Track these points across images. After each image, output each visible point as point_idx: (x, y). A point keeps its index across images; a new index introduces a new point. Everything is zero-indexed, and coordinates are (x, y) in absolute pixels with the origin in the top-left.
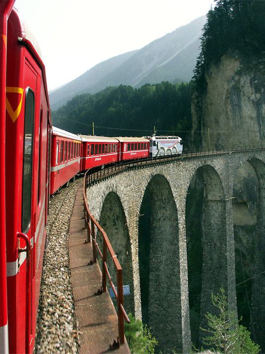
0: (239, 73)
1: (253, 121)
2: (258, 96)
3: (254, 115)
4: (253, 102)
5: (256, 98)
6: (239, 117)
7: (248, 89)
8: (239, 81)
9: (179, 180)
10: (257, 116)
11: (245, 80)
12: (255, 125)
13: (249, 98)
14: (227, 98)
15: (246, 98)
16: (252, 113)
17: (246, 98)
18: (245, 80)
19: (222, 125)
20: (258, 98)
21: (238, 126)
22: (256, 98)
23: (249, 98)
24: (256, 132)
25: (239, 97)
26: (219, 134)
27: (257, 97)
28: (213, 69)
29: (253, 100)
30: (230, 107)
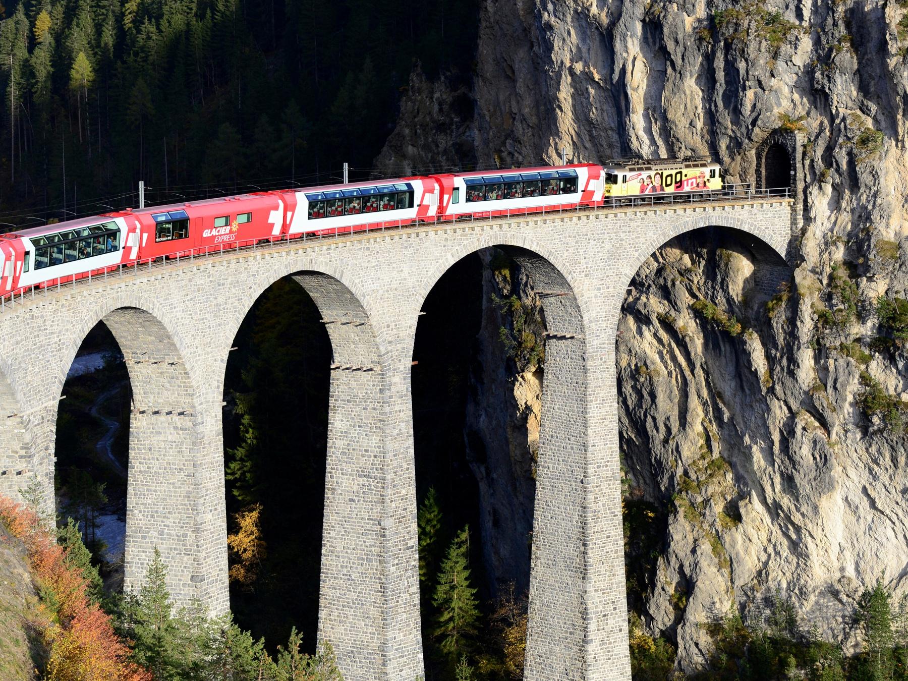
19: (520, 84)
24: (611, 129)
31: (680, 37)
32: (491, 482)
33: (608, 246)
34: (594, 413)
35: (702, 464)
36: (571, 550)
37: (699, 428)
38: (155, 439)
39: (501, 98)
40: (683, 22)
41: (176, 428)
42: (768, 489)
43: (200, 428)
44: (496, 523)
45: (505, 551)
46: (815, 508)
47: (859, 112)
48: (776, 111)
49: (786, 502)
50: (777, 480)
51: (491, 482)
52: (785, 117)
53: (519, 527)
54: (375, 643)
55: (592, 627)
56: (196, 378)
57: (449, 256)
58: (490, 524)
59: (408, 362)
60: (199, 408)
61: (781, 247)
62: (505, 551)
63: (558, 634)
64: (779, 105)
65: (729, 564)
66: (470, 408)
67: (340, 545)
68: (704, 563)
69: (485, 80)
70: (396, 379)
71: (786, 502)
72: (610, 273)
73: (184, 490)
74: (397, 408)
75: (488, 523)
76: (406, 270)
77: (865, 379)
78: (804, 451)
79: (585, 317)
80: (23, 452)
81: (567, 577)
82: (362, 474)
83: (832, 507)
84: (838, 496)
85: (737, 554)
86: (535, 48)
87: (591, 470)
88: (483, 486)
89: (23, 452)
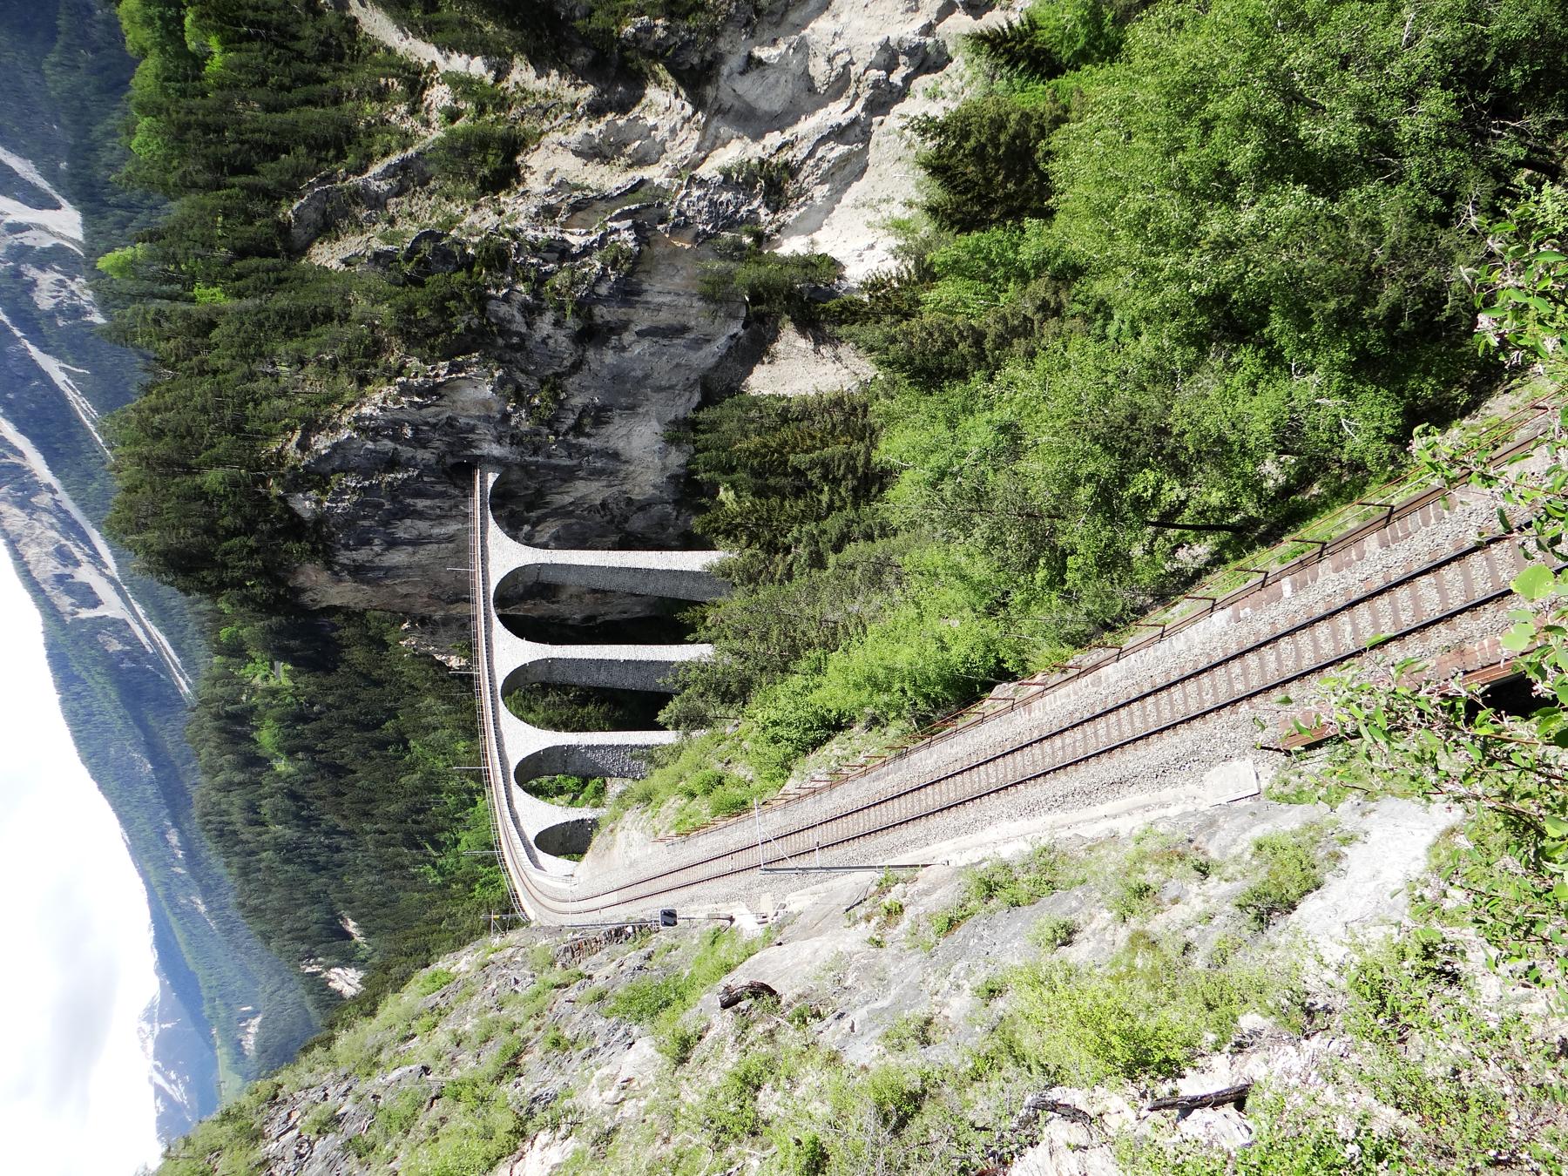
0: (329, 565)
2: (376, 541)
3: (410, 549)
4: (386, 550)
7: (362, 555)
8: (343, 566)
9: (522, 739)
11: (344, 557)
13: (378, 555)
14: (368, 583)
18: (344, 557)
23: (378, 555)
25: (373, 569)
26: (429, 596)
28: (306, 598)
30: (388, 582)
46: (626, 462)
49: (622, 475)
59: (548, 647)
71: (622, 475)
77: (566, 434)
78: (599, 465)
88: (608, 618)
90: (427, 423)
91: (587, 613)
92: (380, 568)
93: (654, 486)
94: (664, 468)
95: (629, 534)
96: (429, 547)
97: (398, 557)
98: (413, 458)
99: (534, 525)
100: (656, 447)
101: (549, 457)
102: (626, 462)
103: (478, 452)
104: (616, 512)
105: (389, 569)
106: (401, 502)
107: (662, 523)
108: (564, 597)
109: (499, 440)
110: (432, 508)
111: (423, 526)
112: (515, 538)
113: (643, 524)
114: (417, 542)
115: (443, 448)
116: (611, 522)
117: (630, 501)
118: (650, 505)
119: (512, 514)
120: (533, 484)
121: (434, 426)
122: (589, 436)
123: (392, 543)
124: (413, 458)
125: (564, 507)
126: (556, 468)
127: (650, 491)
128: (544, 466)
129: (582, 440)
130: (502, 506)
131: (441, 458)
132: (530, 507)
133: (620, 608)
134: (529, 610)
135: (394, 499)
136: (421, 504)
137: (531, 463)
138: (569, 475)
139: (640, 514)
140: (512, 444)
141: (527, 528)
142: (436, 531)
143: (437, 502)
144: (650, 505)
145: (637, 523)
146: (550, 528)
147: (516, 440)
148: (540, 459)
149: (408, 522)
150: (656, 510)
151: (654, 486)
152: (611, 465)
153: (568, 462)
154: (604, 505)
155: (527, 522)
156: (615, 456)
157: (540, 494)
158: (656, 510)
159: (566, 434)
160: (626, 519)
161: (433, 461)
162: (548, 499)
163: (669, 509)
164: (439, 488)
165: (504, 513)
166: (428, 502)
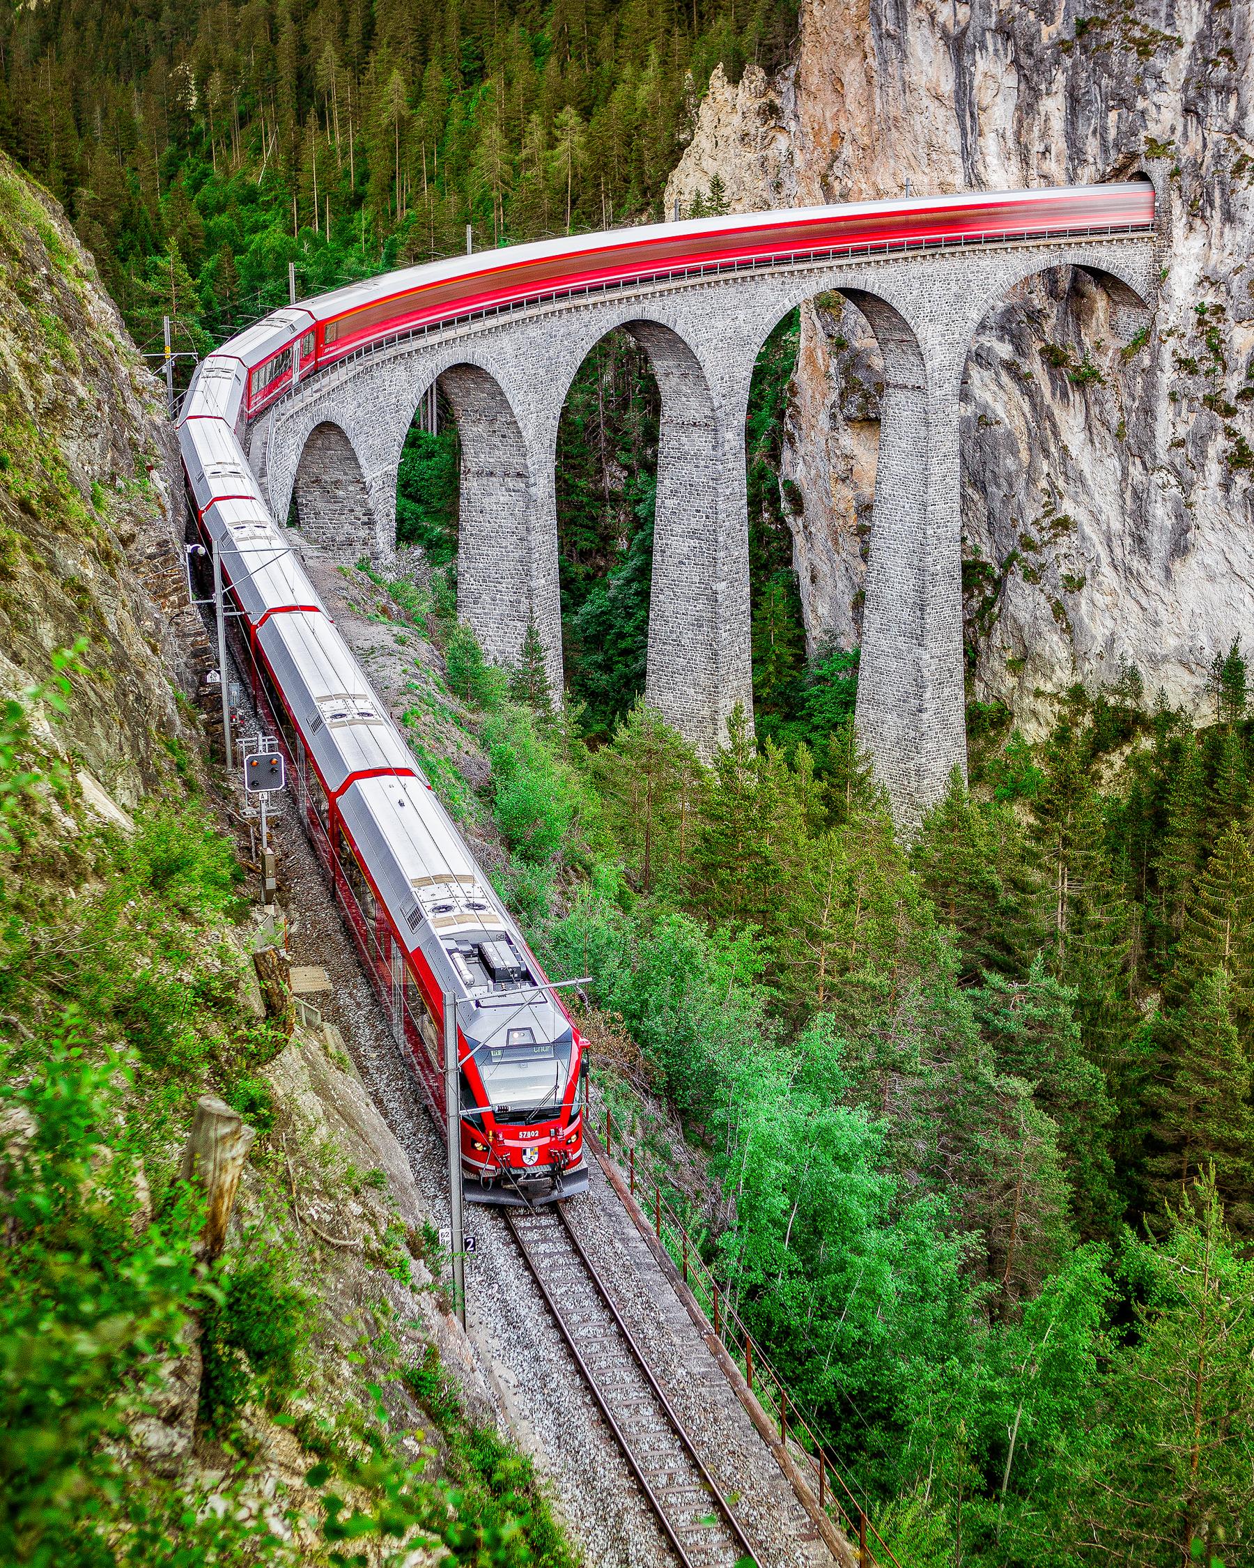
1: (943, 110)
4: (945, 36)
5: (957, 23)
6: (899, 84)
10: (956, 92)
12: (949, 128)
13: (932, 16)
15: (921, 13)
16: (943, 79)
17: (921, 13)
20: (963, 24)
21: (895, 119)
22: (957, 23)
23: (932, 16)
26: (839, 136)
27: (960, 17)
29: (944, 29)
30: (870, 42)
31: (1036, 48)
32: (809, 537)
33: (955, 288)
34: (936, 470)
35: (1046, 522)
36: (905, 615)
37: (1043, 484)
38: (486, 500)
39: (828, 115)
40: (1039, 31)
41: (508, 490)
42: (1118, 551)
43: (533, 490)
44: (813, 579)
45: (823, 610)
46: (1168, 572)
47: (1235, 136)
48: (1143, 135)
49: (1137, 564)
50: (1128, 541)
51: (809, 537)
52: (1151, 142)
53: (839, 584)
54: (706, 712)
55: (927, 695)
56: (528, 434)
57: (786, 301)
58: (808, 580)
60: (531, 469)
61: (1139, 285)
62: (823, 610)
63: (890, 701)
64: (1146, 128)
65: (1069, 630)
66: (786, 455)
67: (669, 609)
68: (1044, 628)
69: (809, 93)
70: (729, 435)
71: (1137, 564)
72: (955, 317)
73: (517, 555)
74: (730, 466)
75: (805, 581)
76: (741, 317)
77: (1230, 433)
78: (1161, 513)
79: (928, 366)
80: (365, 519)
81: (901, 643)
82: (693, 534)
83: (1189, 571)
84: (1192, 560)
85: (1081, 620)
86: (870, 60)
87: (930, 532)
88: (799, 540)
89: (365, 519)
90: (1242, 113)
91: (811, 497)
92: (901, 21)
93: (1111, 641)
94: (1155, 661)
95: (999, 584)
96: (954, 130)
97: (928, 64)
98: (1161, 85)
99: (1011, 367)
100: (1203, 640)
101: (1173, 397)
102: (1168, 572)
103: (1179, 230)
104: (1048, 555)
105: (898, 40)
106: (1057, 62)
107: (1022, 662)
108: (848, 440)
109: (1208, 281)
110: (1044, 135)
111: (1000, 113)
112: (982, 327)
113: (1024, 617)
114: (965, 105)
115: (1186, 153)
116: (1028, 545)
117: (1074, 584)
118: (1069, 630)
119: (1035, 317)
120: (1105, 363)
121: (1238, 130)
122: (1226, 486)
123: (958, 46)
124: (1161, 85)
125: (1056, 434)
126: (1148, 411)
127: (1098, 629)
128: (1151, 386)
129: (1214, 471)
130: (1053, 293)
131: (1157, 148)
132: (1054, 358)
133: (824, 568)
134: (811, 359)
135: (1063, 47)
136: (1054, 106)
137: (1155, 357)
138: (1132, 443)
139: (1046, 610)
140: (1201, 310)
141: (1004, 350)
142: (990, 144)
143: (1059, 144)
144: (1069, 630)
145: (1024, 602)
146: (1003, 403)
147: (1208, 321)
148: (1168, 377)
149: (1011, 80)
150: (1053, 645)
151: (1111, 641)
152: (1159, 543)
153: (1163, 433)
154: (1064, 524)
155: (1019, 350)
156: (1180, 549)
157: (1084, 380)
158: (1053, 645)
159: (1230, 433)
160: (1032, 576)
161: (1154, 130)
162: (1075, 397)
163: (1065, 677)
164: (1092, 147)
165: (1039, 300)
166: (1058, 124)
